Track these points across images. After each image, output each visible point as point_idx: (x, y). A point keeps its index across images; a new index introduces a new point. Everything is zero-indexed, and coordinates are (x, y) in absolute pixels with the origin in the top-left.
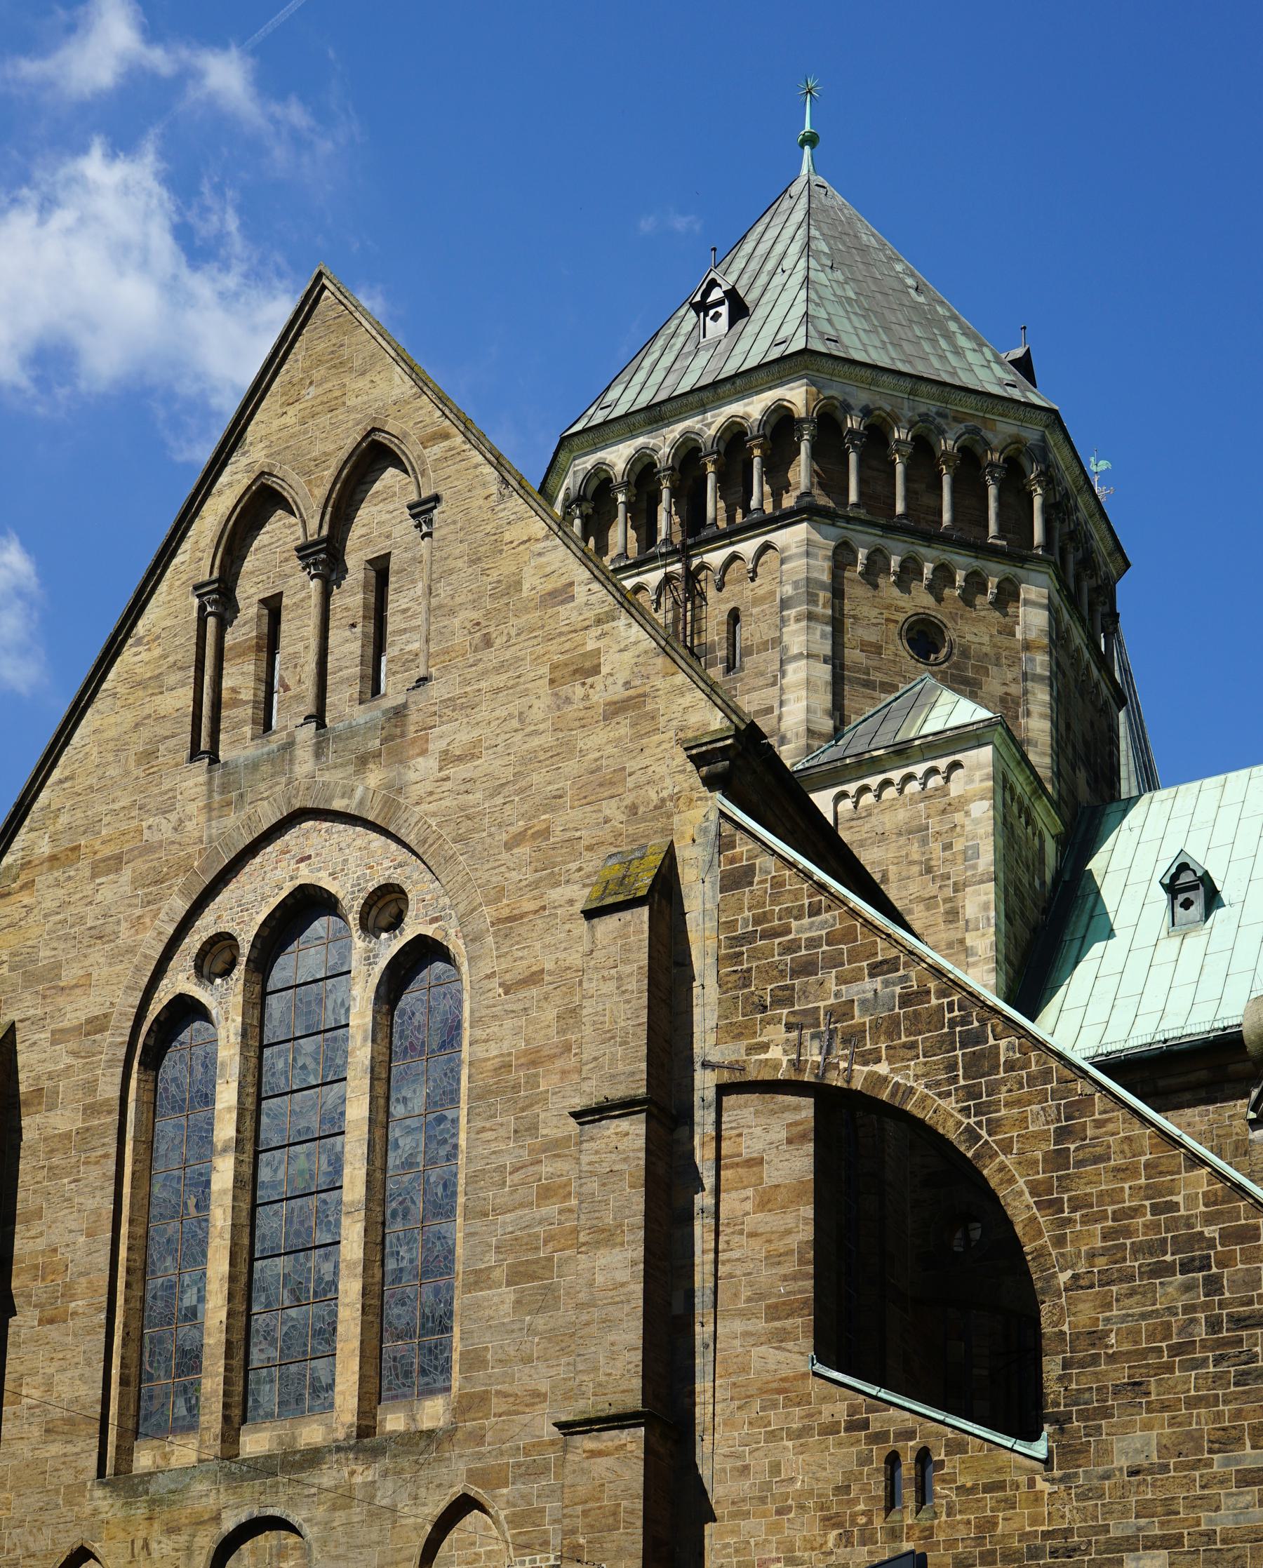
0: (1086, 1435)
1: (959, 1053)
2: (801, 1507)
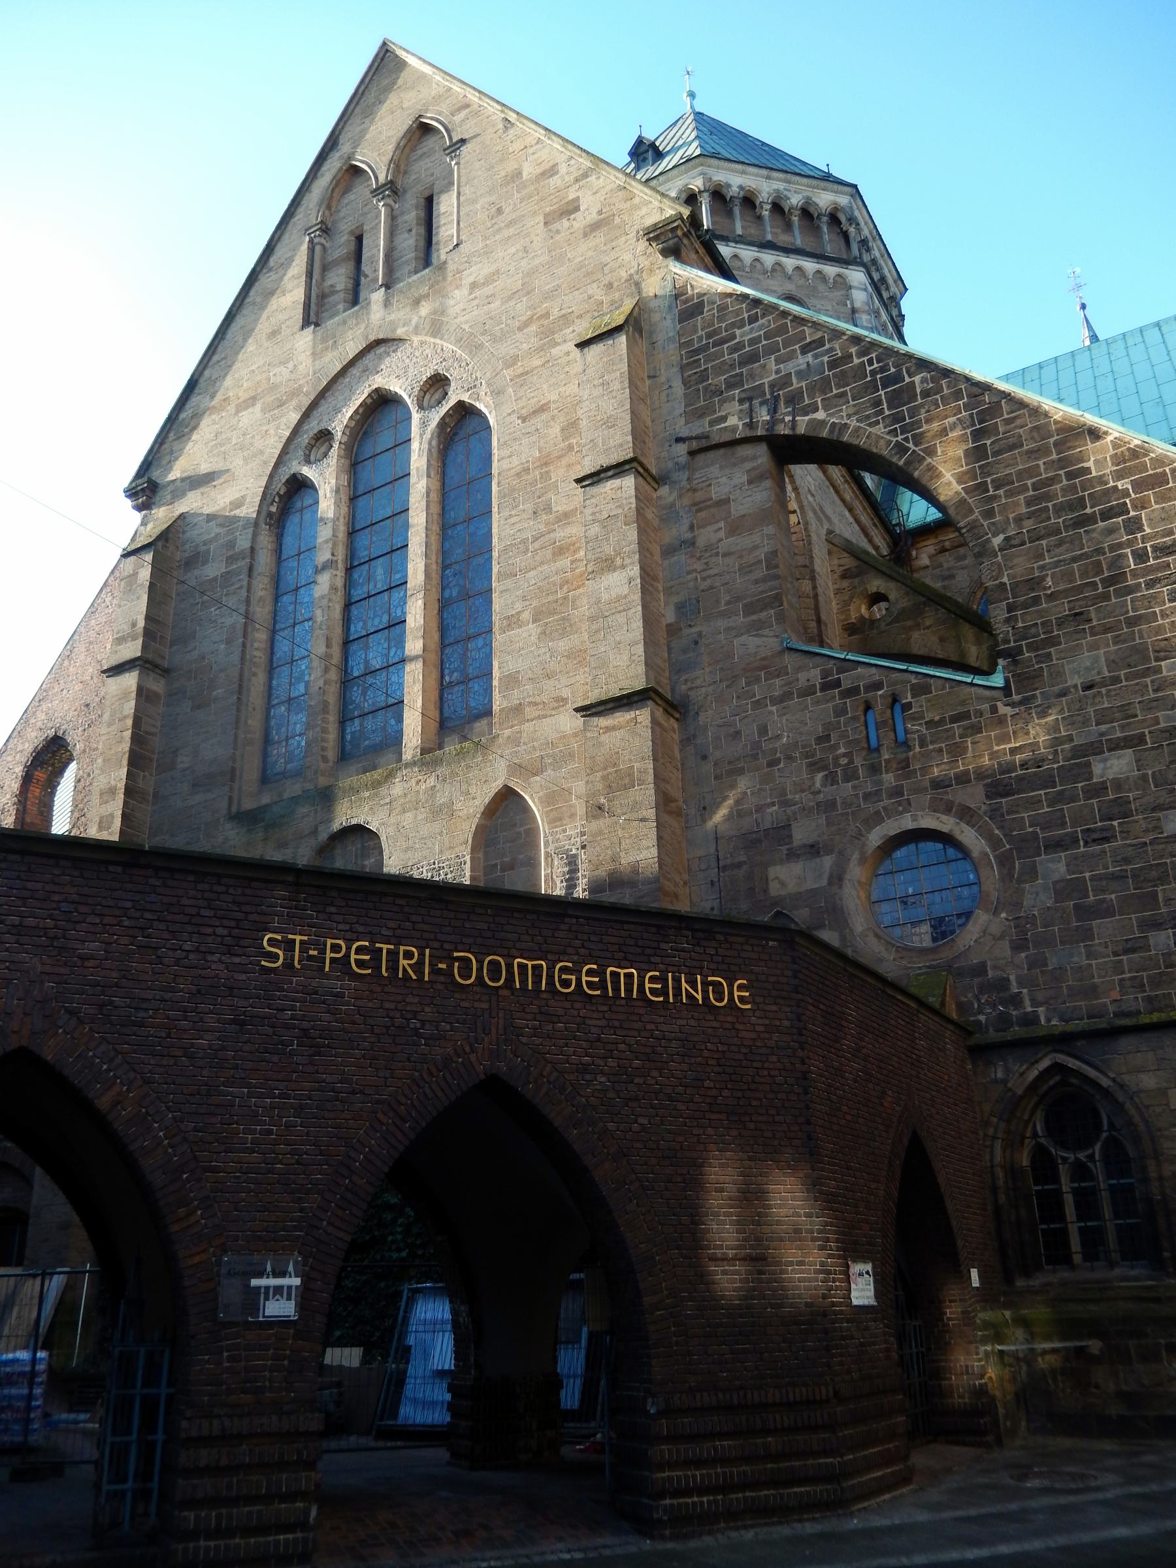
0: (1037, 663)
1: (882, 392)
2: (789, 758)
